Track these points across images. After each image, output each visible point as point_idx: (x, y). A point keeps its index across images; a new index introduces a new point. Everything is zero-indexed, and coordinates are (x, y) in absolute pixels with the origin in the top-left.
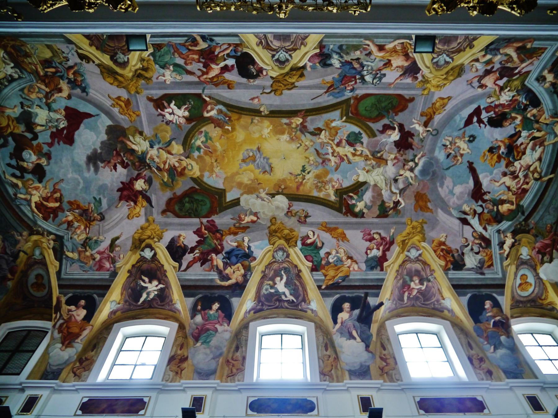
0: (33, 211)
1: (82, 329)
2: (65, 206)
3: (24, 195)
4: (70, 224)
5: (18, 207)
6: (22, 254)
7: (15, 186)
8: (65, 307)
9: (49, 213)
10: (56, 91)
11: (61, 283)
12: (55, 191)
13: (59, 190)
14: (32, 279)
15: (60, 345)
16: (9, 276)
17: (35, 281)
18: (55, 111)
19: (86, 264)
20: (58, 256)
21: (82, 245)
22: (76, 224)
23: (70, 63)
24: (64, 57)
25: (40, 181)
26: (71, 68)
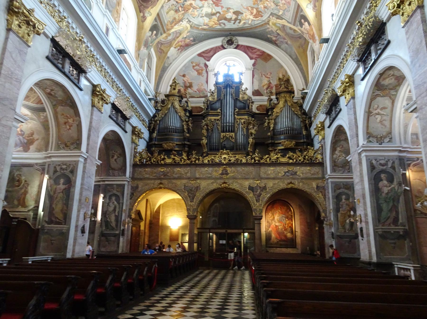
0: (258, 20)
1: (312, 30)
2: (256, 6)
3: (249, 21)
4: (265, 7)
5: (255, 25)
6: (277, 31)
7: (245, 23)
8: (302, 29)
9: (259, 14)
10: (192, 6)
11: (293, 23)
12: (248, 9)
13: (247, 7)
14: (291, 32)
15: (314, 44)
16: (286, 41)
17: (292, 31)
18: (203, 5)
19: (286, 9)
20: (280, 18)
21: (277, 6)
22: (265, 5)
23: (175, 3)
24: (172, 6)
25: (242, 14)
26: (177, 2)
